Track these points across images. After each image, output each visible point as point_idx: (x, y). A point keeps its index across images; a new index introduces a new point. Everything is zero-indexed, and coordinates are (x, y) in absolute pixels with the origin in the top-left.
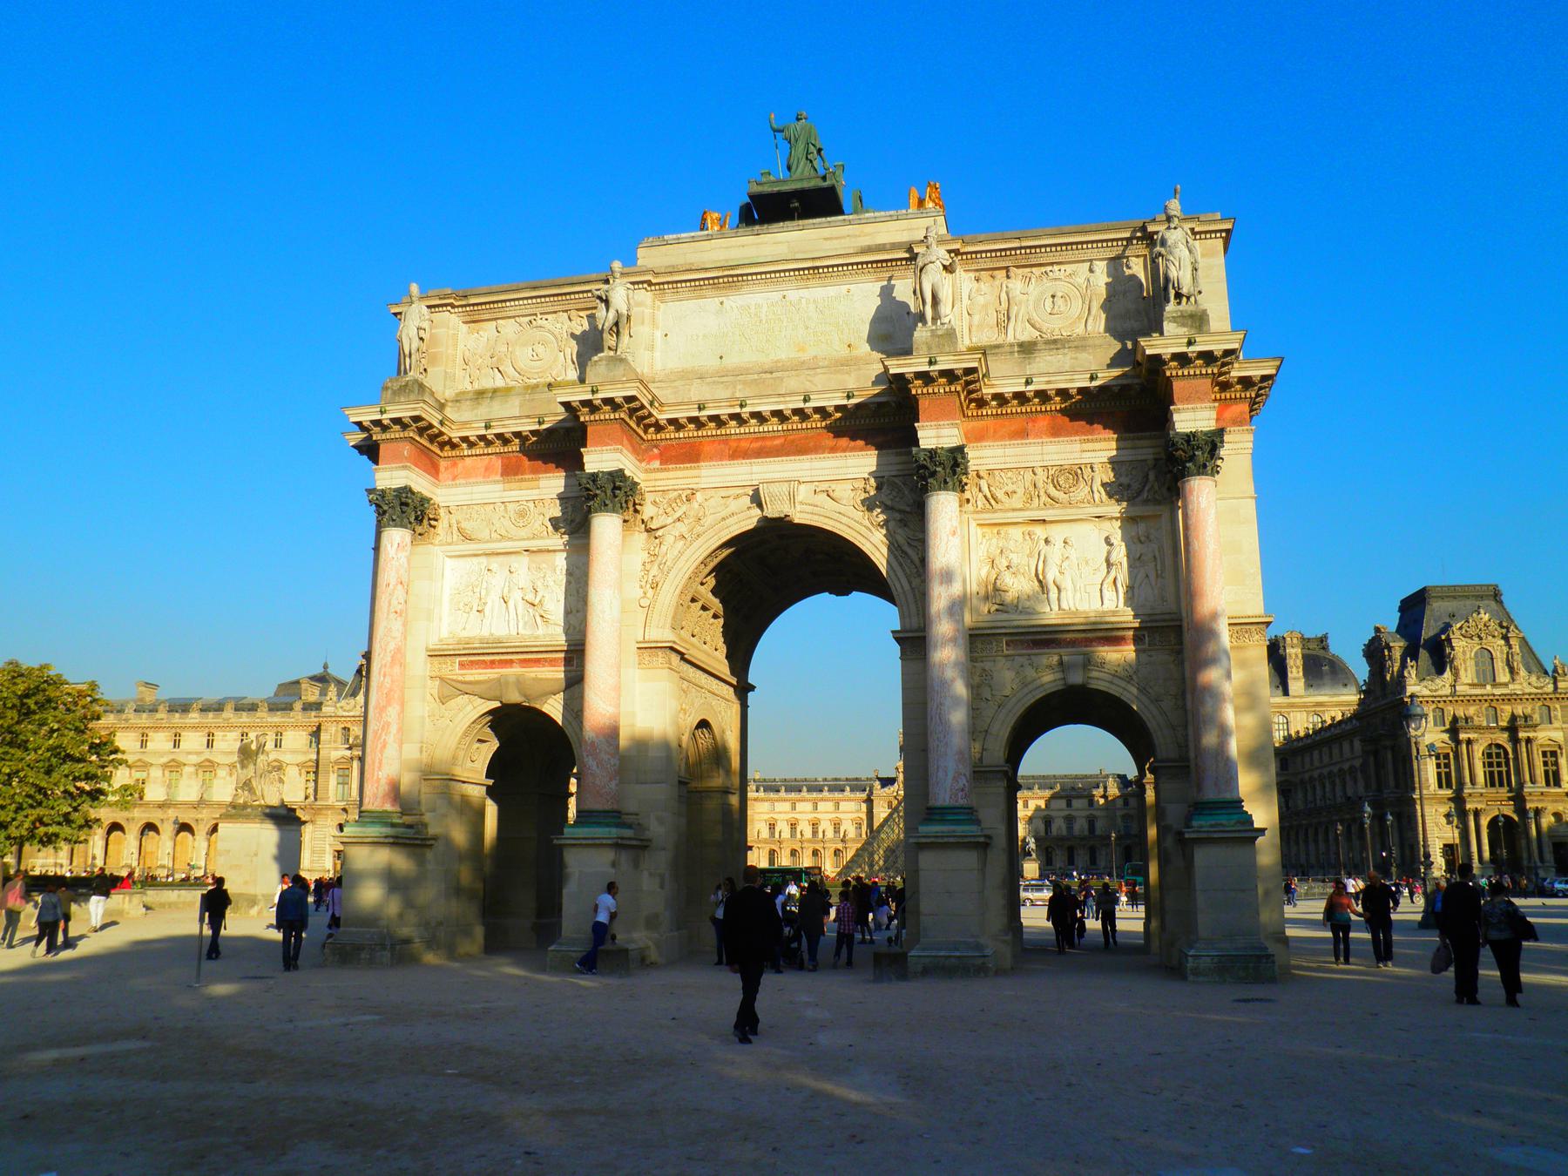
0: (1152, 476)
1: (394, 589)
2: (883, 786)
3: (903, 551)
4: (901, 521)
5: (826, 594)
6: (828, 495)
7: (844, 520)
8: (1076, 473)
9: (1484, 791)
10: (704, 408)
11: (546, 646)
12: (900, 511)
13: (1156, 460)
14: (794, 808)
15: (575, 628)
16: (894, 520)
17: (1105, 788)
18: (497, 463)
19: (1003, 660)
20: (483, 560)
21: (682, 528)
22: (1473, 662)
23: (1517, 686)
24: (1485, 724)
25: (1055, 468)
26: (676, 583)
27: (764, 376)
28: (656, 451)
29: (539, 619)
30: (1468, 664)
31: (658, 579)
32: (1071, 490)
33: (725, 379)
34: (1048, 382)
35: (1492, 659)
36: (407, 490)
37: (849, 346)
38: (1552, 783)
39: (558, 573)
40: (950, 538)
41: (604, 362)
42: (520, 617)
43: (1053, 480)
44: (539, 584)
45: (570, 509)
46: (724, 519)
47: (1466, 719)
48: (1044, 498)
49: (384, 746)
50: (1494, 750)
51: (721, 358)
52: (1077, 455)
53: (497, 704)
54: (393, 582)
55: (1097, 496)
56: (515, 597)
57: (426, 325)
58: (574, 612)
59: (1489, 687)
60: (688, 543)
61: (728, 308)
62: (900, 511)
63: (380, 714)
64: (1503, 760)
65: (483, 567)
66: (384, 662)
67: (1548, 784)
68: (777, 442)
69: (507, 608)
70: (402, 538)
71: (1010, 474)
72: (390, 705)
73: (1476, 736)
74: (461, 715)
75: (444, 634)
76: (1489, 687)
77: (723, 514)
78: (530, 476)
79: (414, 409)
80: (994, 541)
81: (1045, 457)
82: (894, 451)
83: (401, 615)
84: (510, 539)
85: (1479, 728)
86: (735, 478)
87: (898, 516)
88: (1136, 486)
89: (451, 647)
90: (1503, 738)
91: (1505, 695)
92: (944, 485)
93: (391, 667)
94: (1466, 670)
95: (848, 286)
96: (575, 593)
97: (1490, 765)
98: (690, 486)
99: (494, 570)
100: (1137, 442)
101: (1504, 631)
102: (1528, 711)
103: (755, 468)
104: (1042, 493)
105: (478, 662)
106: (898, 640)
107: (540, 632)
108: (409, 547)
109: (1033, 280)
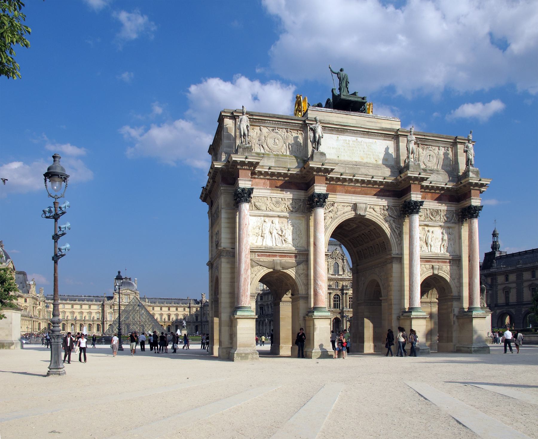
0: (455, 216)
2: (108, 300)
6: (373, 210)
7: (378, 218)
8: (437, 212)
9: (333, 310)
11: (289, 251)
13: (456, 211)
14: (72, 307)
15: (296, 245)
17: (190, 304)
20: (262, 218)
21: (331, 215)
22: (333, 266)
23: (344, 276)
24: (335, 288)
26: (330, 233)
29: (283, 241)
30: (332, 267)
32: (436, 217)
35: (338, 266)
38: (351, 308)
42: (277, 240)
43: (431, 213)
44: (283, 228)
46: (344, 213)
47: (346, 286)
48: (429, 218)
50: (336, 296)
52: (437, 207)
53: (272, 270)
55: (441, 219)
56: (275, 232)
58: (295, 239)
59: (337, 275)
63: (247, 272)
64: (338, 300)
65: (262, 220)
67: (350, 308)
73: (332, 291)
74: (259, 273)
76: (337, 275)
77: (342, 212)
81: (430, 206)
84: (273, 211)
85: (333, 289)
86: (346, 200)
88: (450, 218)
89: (254, 248)
90: (339, 293)
91: (341, 278)
94: (331, 269)
97: (335, 301)
98: (333, 201)
99: (267, 222)
100: (452, 205)
101: (343, 257)
102: (347, 284)
103: (353, 198)
104: (429, 216)
105: (264, 255)
107: (284, 245)
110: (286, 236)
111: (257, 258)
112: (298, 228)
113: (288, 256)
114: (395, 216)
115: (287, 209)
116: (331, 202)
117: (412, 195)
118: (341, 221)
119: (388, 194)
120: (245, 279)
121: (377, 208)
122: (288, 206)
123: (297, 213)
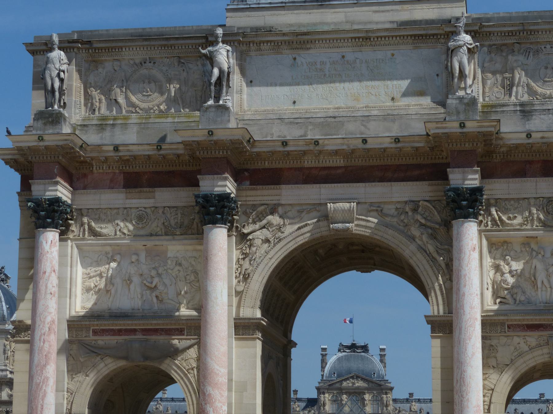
1: (49, 276)
3: (433, 257)
4: (432, 234)
5: (354, 272)
10: (286, 144)
12: (431, 228)
16: (428, 234)
18: (121, 177)
19: (506, 339)
25: (545, 200)
27: (329, 120)
28: (246, 174)
29: (155, 300)
31: (249, 271)
33: (299, 120)
34: (543, 138)
36: (57, 200)
37: (393, 99)
39: (169, 262)
40: (472, 252)
41: (213, 109)
45: (179, 215)
49: (45, 395)
51: (294, 102)
53: (122, 363)
54: (48, 270)
57: (64, 67)
60: (272, 244)
61: (299, 63)
62: (431, 228)
65: (110, 256)
66: (43, 332)
68: (339, 171)
69: (129, 290)
70: (54, 236)
71: (512, 202)
72: (48, 364)
75: (78, 309)
78: (148, 189)
79: (66, 140)
80: (500, 250)
82: (427, 182)
83: (54, 296)
87: (430, 231)
92: (466, 216)
93: (49, 335)
95: (392, 52)
96: (184, 279)
103: (323, 191)
106: (428, 322)
108: (58, 244)
109: (531, 54)
110: (161, 288)
111: (92, 337)
112: (191, 269)
113: (162, 330)
114: (437, 223)
115: (161, 229)
116: (266, 206)
117: (451, 176)
118: (292, 246)
119: (416, 173)
120: (39, 385)
121: (390, 209)
122: (164, 223)
123: (186, 236)
